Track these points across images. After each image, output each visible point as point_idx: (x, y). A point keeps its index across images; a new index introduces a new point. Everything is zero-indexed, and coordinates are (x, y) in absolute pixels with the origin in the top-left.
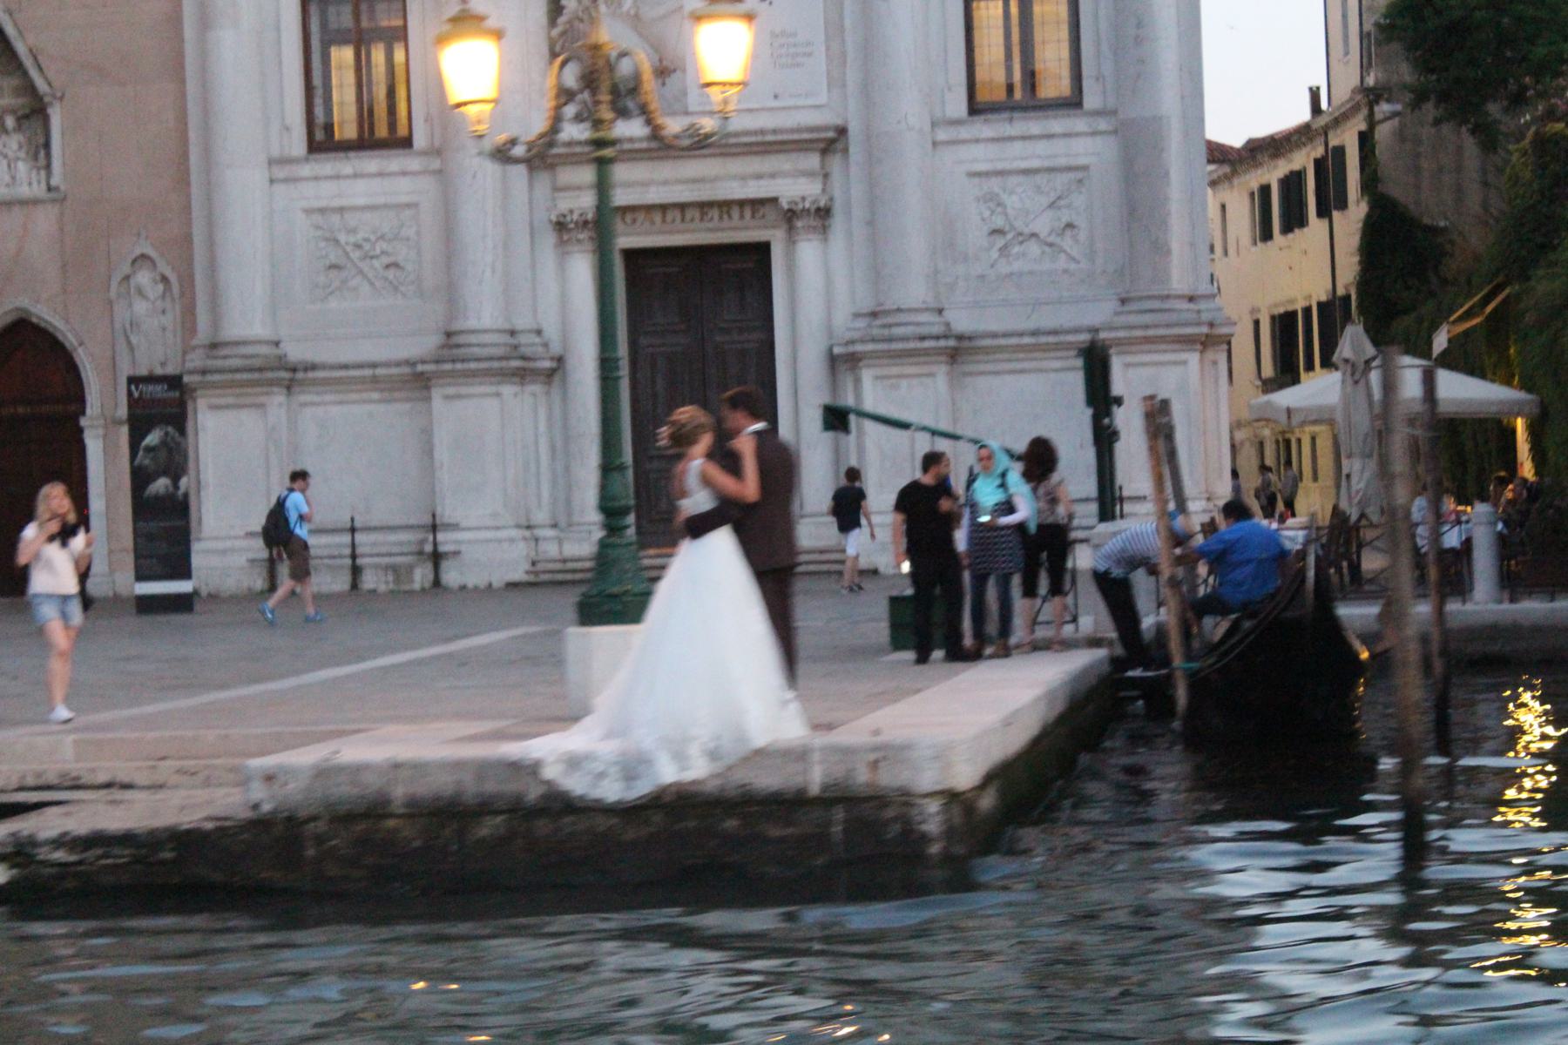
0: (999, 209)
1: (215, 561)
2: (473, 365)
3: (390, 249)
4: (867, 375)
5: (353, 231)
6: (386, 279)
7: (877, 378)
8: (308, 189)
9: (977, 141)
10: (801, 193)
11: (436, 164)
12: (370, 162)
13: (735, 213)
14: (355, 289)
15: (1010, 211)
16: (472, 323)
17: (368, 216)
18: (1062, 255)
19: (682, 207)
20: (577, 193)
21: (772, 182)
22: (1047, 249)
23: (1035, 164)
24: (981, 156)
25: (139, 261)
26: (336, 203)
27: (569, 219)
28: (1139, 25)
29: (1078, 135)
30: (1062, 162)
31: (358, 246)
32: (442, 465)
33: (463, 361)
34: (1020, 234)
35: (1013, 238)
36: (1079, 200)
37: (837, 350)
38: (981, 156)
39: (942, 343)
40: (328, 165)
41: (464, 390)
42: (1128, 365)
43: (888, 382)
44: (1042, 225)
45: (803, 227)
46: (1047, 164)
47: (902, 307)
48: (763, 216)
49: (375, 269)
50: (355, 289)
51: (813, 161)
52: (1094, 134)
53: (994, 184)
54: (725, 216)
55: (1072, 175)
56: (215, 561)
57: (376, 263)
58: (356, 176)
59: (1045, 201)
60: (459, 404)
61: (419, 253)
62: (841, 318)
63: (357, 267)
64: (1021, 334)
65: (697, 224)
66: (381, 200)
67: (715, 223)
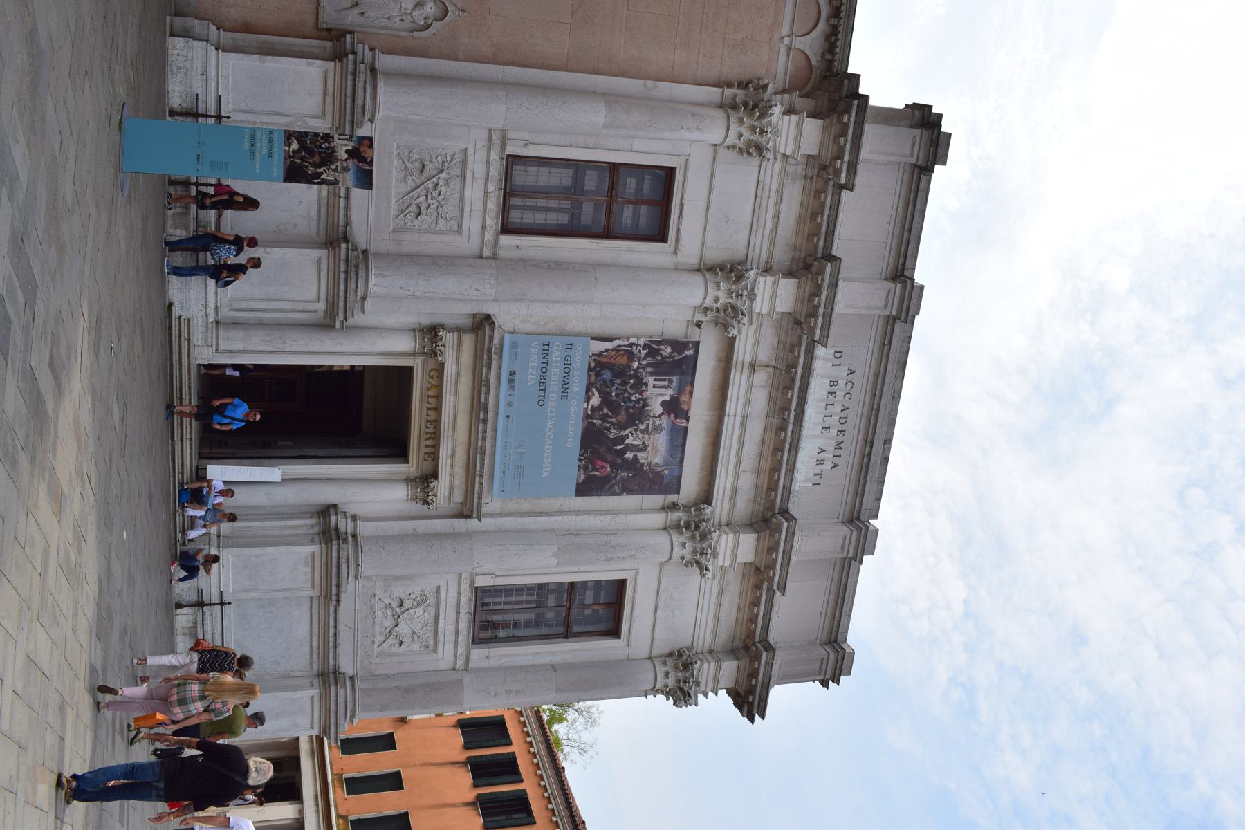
0: (415, 603)
1: (198, 64)
2: (342, 287)
3: (430, 210)
4: (315, 548)
5: (447, 184)
6: (410, 205)
7: (313, 554)
8: (481, 155)
9: (459, 593)
10: (438, 495)
11: (487, 253)
12: (493, 205)
13: (428, 443)
14: (405, 180)
15: (413, 610)
16: (373, 280)
17: (457, 195)
18: (383, 638)
19: (438, 409)
20: (455, 347)
21: (448, 474)
22: (389, 630)
23: (441, 625)
24: (449, 595)
25: (443, 7)
26: (469, 174)
27: (439, 343)
28: (517, 692)
29: (456, 647)
30: (441, 638)
31: (436, 186)
32: (269, 253)
33: (346, 280)
34: (399, 617)
35: (396, 612)
36: (416, 647)
37: (333, 518)
38: (449, 595)
39: (334, 598)
40: (496, 171)
41: (324, 274)
42: (312, 698)
43: (310, 558)
44: (403, 629)
45: (416, 492)
46: (441, 631)
47: (360, 567)
48: (425, 460)
49: (418, 197)
50: (405, 180)
51: (458, 497)
52: (455, 656)
53: (432, 600)
54: (428, 436)
55: (431, 643)
56: (198, 64)
57: (422, 199)
58: (486, 192)
59: (418, 629)
60: (314, 270)
61: (427, 231)
62: (352, 509)
63: (421, 185)
64: (335, 627)
65: (425, 418)
66: (467, 209)
67: (424, 429)
